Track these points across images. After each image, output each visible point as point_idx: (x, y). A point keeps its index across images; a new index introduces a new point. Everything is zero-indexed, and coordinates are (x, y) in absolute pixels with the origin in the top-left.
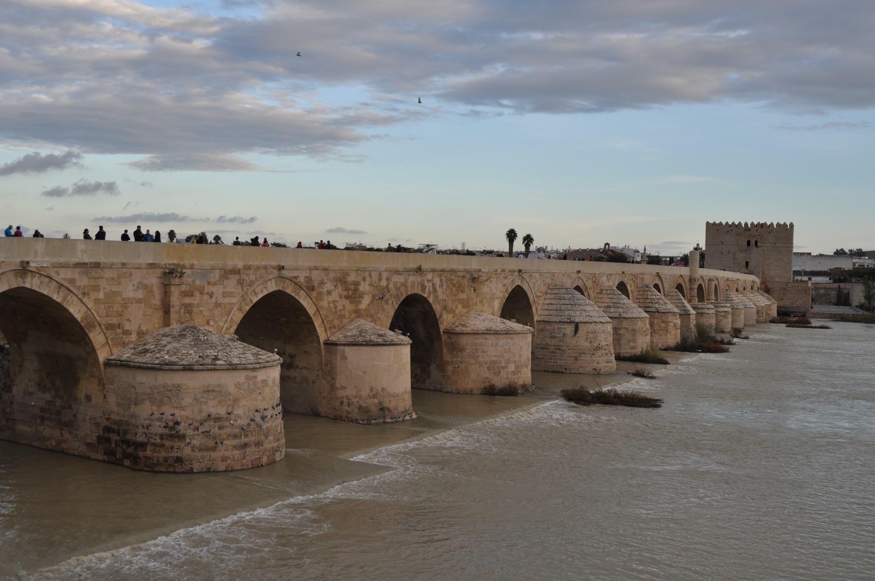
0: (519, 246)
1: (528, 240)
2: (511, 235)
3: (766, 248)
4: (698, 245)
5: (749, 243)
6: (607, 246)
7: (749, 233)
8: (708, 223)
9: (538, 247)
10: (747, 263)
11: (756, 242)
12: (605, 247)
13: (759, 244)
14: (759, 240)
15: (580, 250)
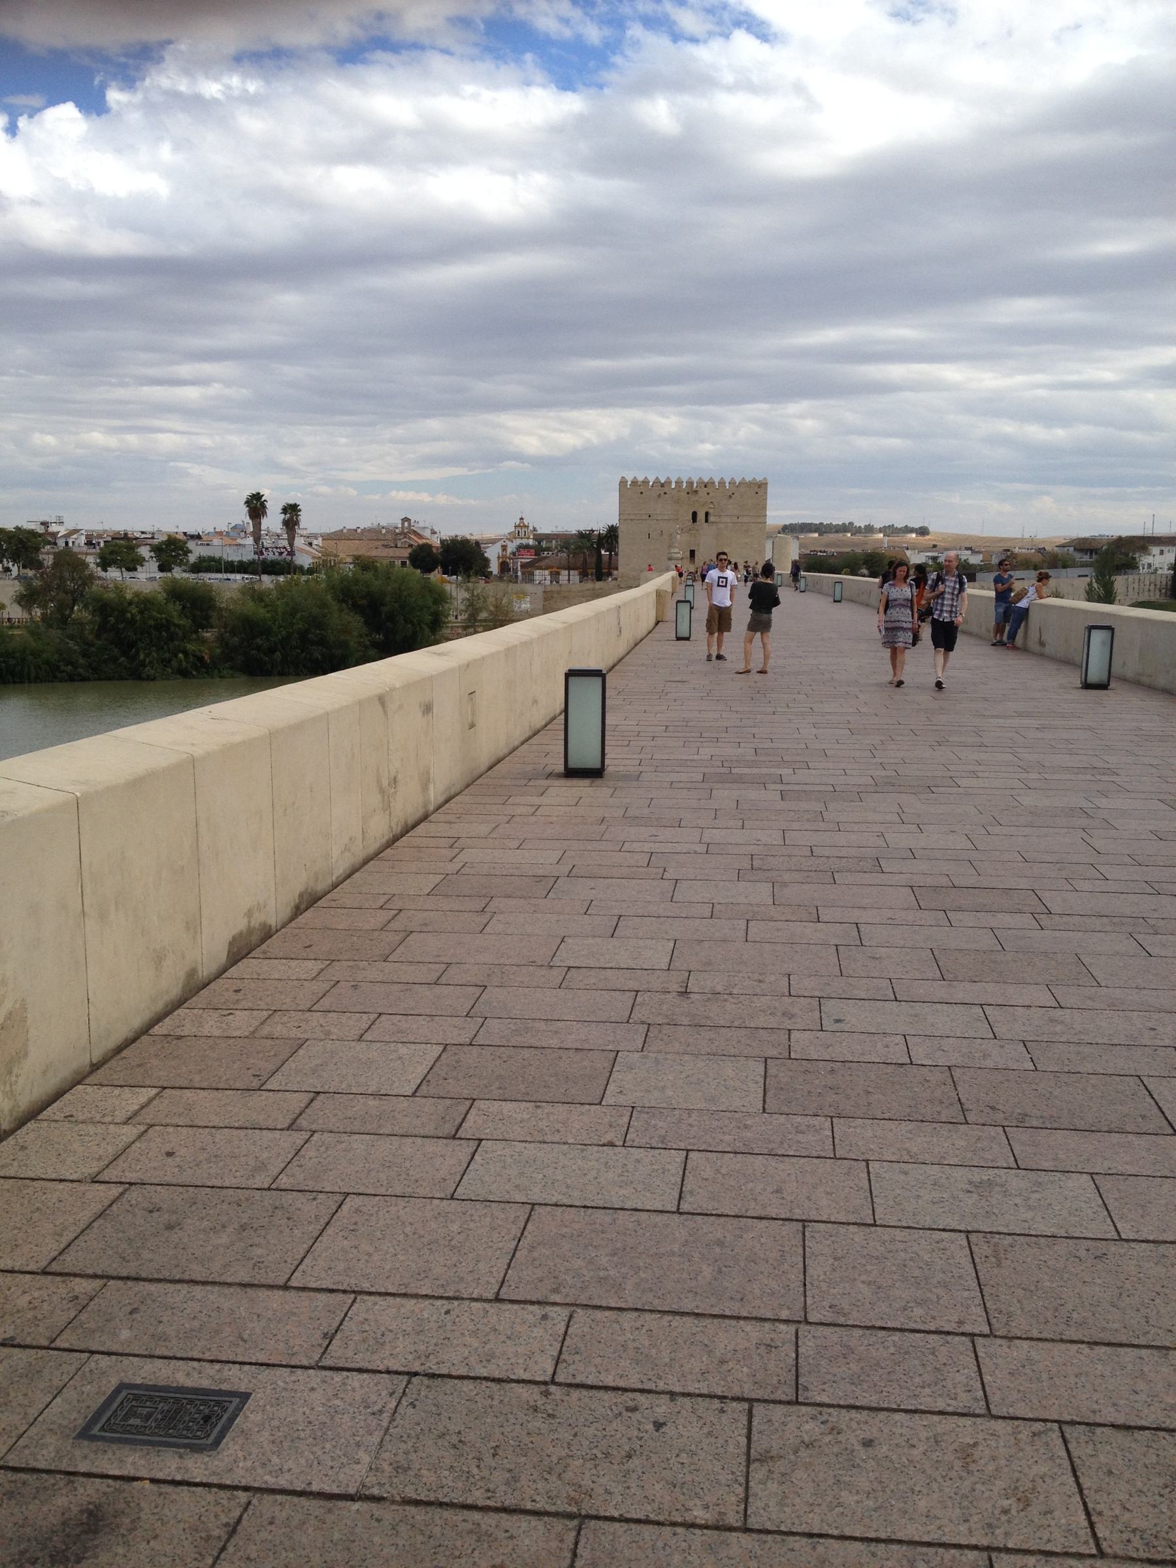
0: (273, 521)
1: (292, 511)
2: (256, 506)
3: (722, 526)
4: (522, 519)
5: (694, 515)
6: (406, 524)
7: (694, 498)
8: (623, 482)
9: (233, 525)
10: (692, 553)
11: (707, 514)
12: (403, 524)
13: (711, 519)
14: (711, 511)
15: (345, 531)
